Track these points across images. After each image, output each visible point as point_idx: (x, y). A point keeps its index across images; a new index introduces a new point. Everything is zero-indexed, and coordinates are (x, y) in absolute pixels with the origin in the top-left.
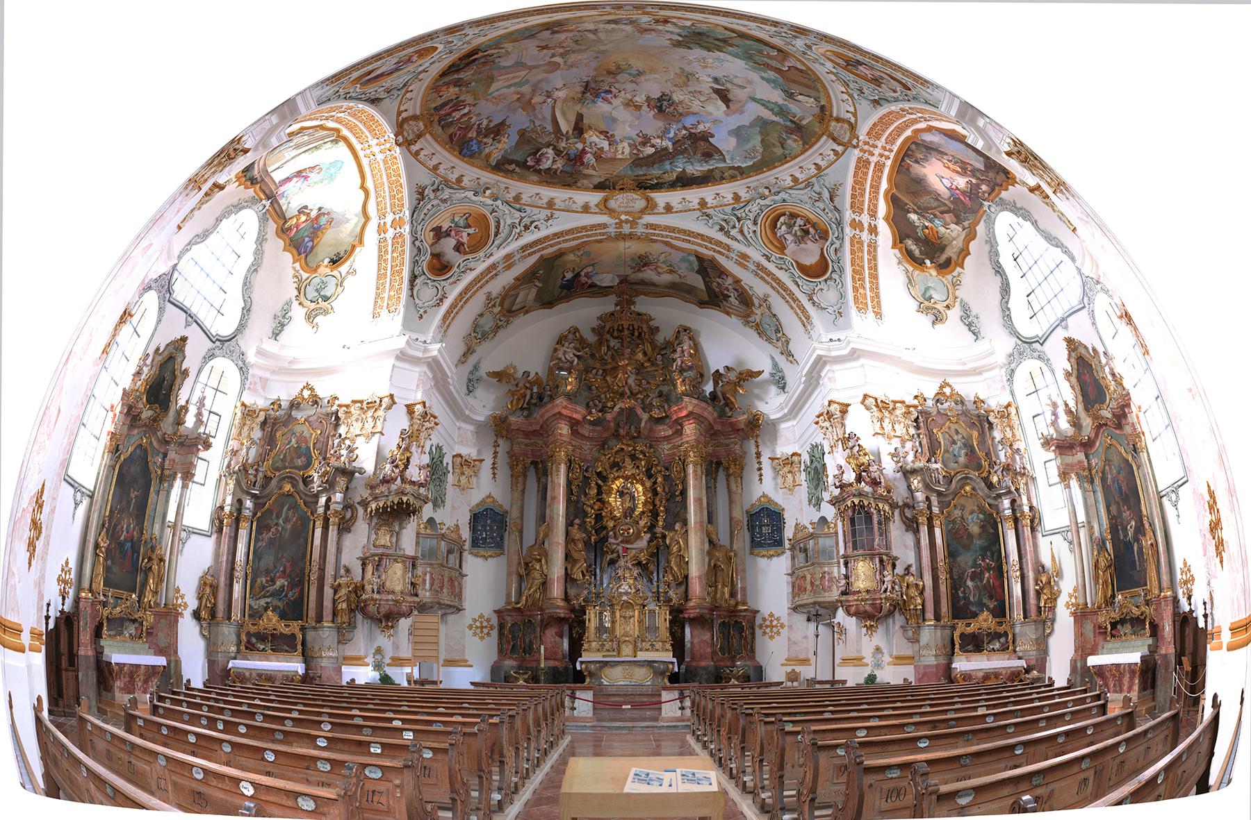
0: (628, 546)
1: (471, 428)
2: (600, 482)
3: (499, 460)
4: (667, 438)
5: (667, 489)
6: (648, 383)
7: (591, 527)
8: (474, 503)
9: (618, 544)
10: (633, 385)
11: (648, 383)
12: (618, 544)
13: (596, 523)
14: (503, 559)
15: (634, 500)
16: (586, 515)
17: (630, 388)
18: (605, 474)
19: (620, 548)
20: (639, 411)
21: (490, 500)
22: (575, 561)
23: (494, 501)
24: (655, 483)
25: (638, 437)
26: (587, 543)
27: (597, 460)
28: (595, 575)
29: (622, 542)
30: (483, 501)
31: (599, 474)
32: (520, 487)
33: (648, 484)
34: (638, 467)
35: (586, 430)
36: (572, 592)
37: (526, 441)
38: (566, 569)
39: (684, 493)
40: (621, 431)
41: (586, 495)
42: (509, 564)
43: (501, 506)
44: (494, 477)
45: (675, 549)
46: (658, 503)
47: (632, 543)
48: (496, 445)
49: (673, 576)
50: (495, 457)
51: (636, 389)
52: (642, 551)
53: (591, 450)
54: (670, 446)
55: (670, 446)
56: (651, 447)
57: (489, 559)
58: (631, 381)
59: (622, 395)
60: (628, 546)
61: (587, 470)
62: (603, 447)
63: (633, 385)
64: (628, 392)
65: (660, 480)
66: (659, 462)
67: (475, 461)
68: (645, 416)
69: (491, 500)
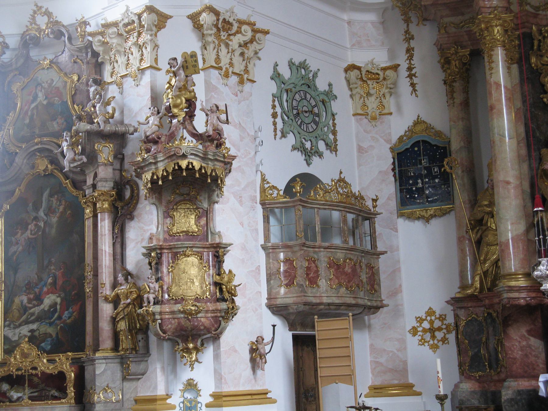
1: (371, 17)
3: (415, 61)
8: (395, 139)
14: (450, 219)
21: (419, 128)
23: (429, 128)
30: (410, 131)
32: (459, 98)
37: (457, 19)
42: (459, 227)
43: (439, 134)
44: (415, 90)
48: (409, 37)
50: (410, 58)
57: (433, 221)
67: (384, 69)
69: (423, 126)
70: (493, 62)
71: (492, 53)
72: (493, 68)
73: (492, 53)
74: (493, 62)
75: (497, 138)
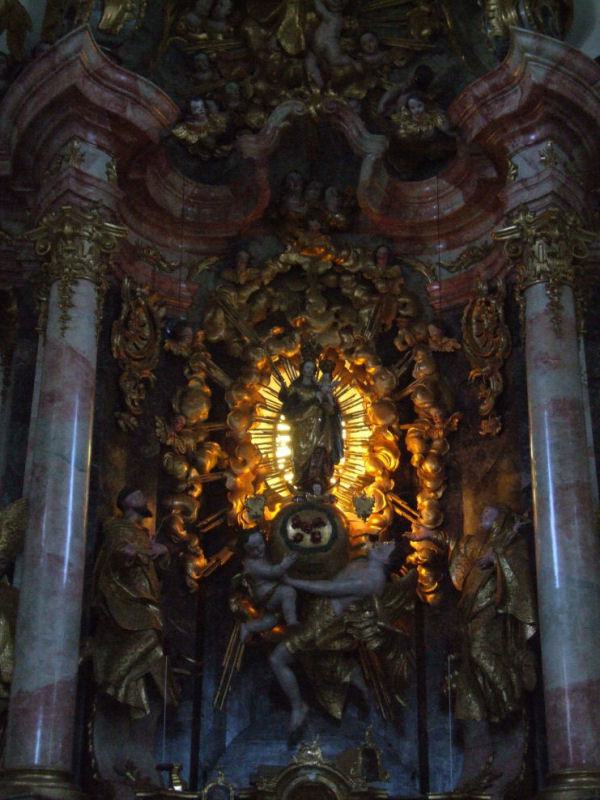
0: (318, 586)
2: (219, 375)
4: (450, 228)
5: (447, 398)
6: (383, 46)
7: (187, 526)
9: (278, 580)
10: (333, 51)
11: (383, 46)
12: (278, 580)
13: (202, 516)
15: (337, 429)
16: (170, 486)
17: (323, 62)
18: (236, 348)
19: (287, 594)
20: (353, 127)
22: (126, 637)
24: (407, 379)
25: (352, 227)
26: (172, 574)
27: (212, 302)
28: (198, 699)
29: (297, 570)
31: (219, 352)
33: (382, 386)
34: (348, 330)
35: (176, 192)
36: (104, 756)
38: (86, 670)
39: (513, 406)
40: (293, 202)
41: (170, 417)
45: (484, 598)
46: (414, 446)
47: (329, 577)
49: (480, 695)
51: (341, 64)
52: (363, 600)
53: (193, 268)
54: (455, 253)
55: (455, 253)
56: (393, 259)
58: (326, 37)
59: (295, 83)
60: (318, 586)
61: (176, 337)
62: (229, 260)
63: (333, 51)
64: (314, 73)
65: (422, 371)
66: (420, 311)
68: (373, 147)
70: (73, 306)
71: (74, 288)
72: (69, 319)
73: (74, 288)
74: (73, 306)
75: (53, 463)
